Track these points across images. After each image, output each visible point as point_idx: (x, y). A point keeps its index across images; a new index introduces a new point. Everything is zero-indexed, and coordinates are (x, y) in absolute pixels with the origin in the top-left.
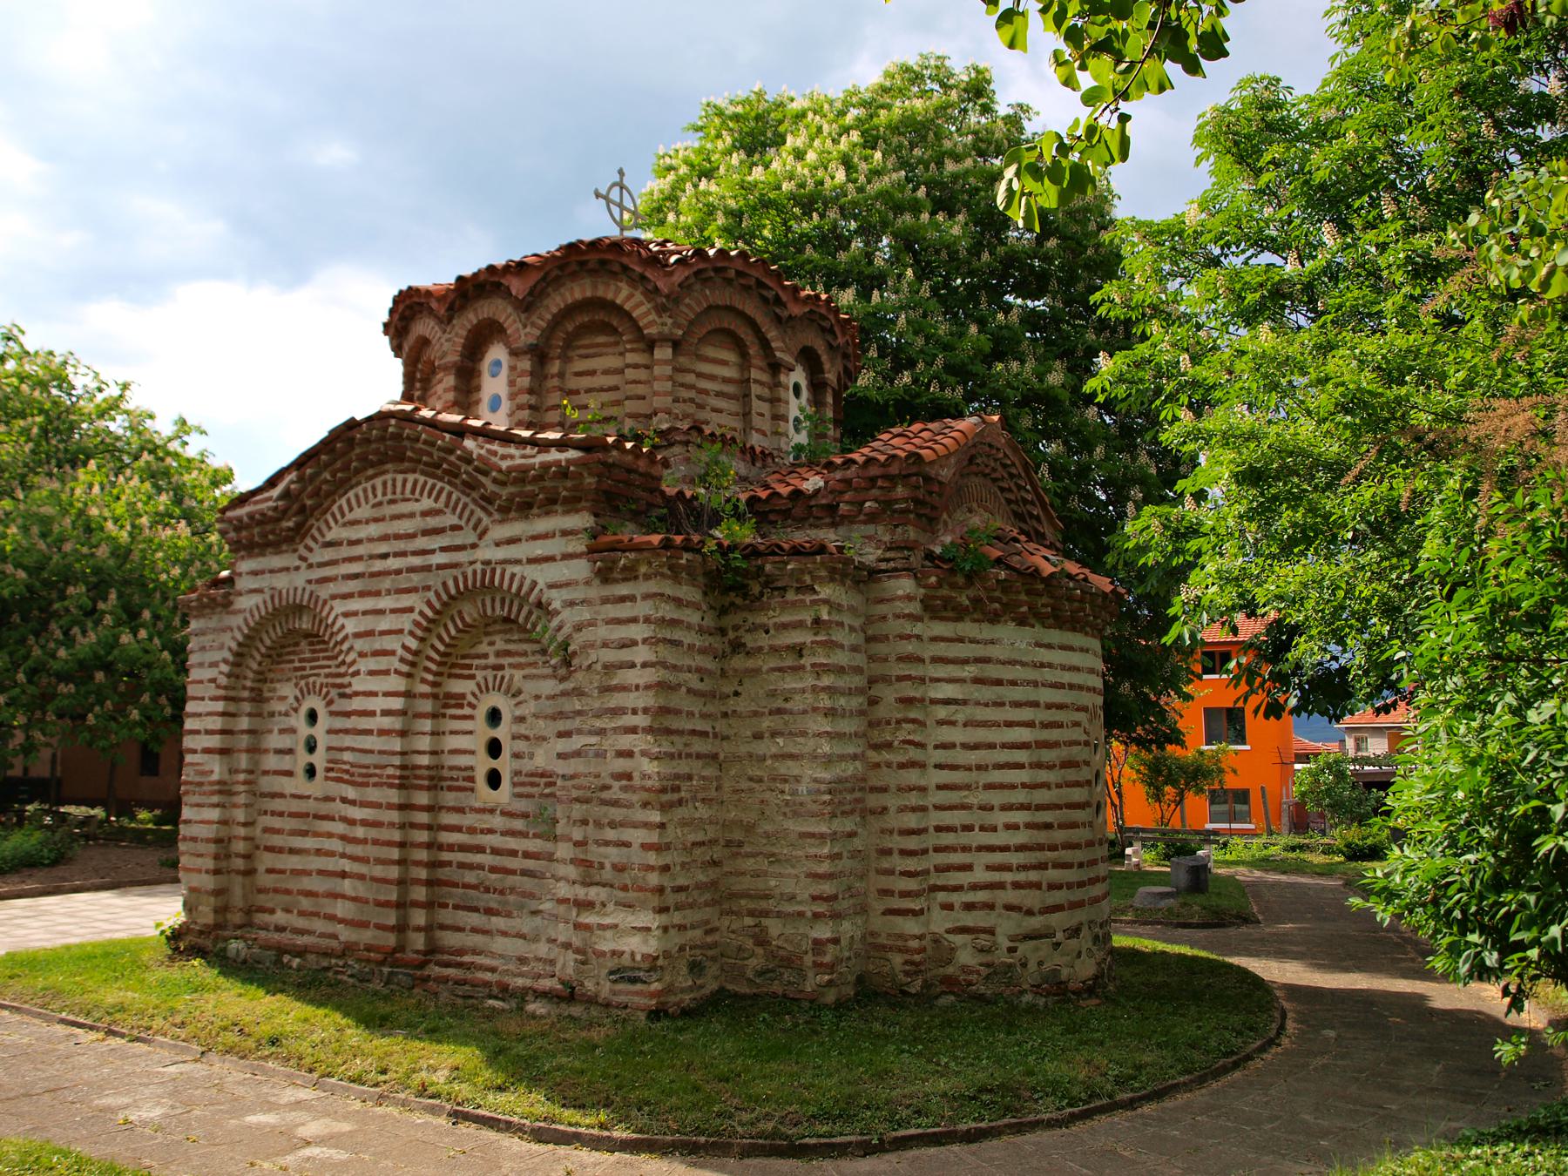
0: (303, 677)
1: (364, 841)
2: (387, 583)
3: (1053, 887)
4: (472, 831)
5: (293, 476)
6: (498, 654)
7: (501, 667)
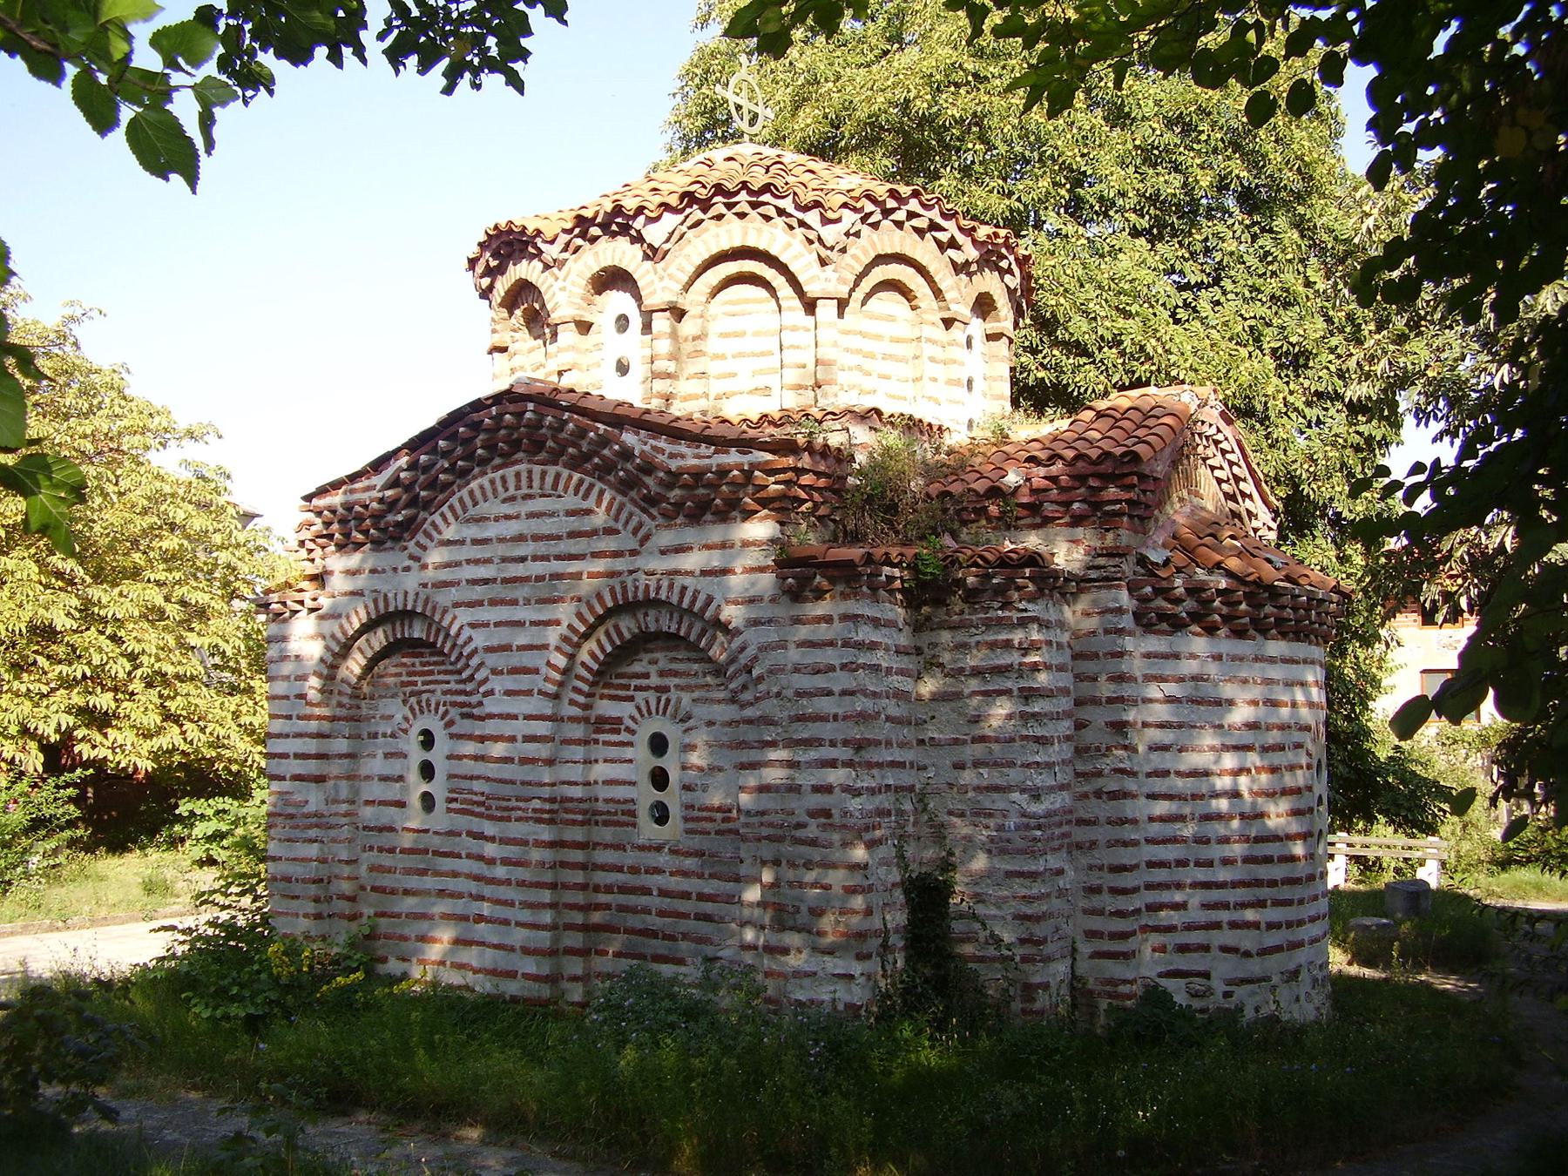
0: (412, 694)
1: (508, 882)
2: (521, 592)
3: (1271, 926)
5: (403, 461)
6: (662, 674)
7: (666, 689)
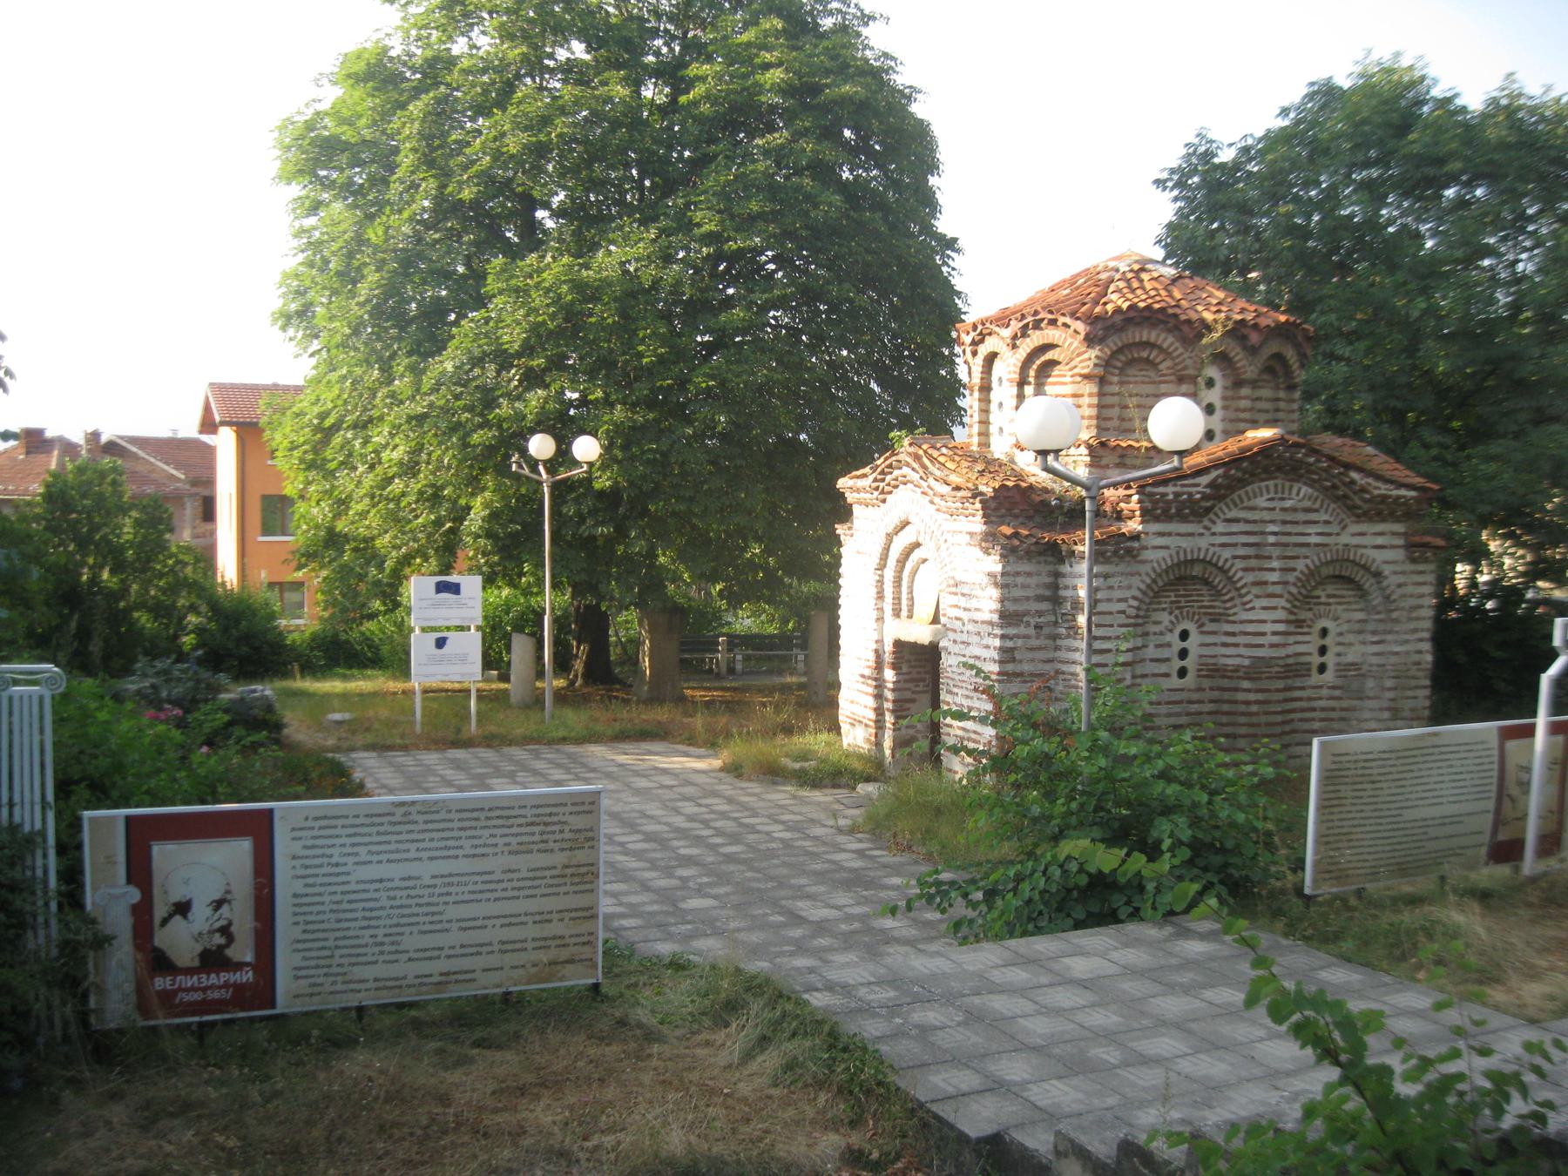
4: (1310, 699)
5: (1220, 471)
6: (1329, 596)
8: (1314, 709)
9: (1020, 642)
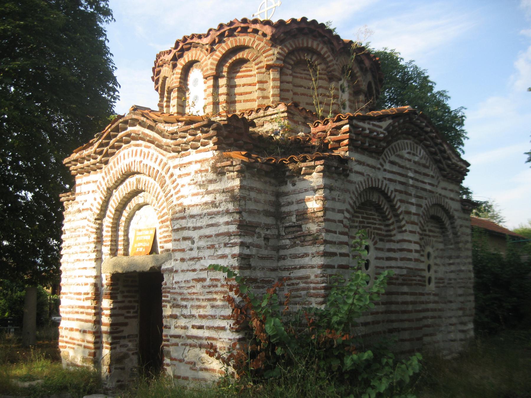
6: (430, 231)
8: (427, 310)
9: (254, 251)
